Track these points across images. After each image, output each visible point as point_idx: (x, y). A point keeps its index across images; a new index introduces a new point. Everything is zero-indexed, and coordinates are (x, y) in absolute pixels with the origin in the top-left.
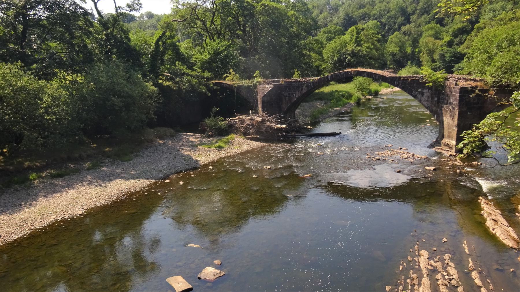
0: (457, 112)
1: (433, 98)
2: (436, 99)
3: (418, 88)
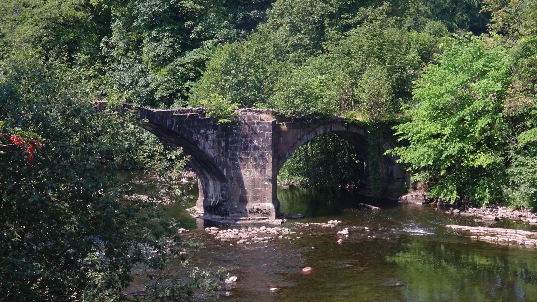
1: (219, 143)
2: (223, 144)
3: (200, 128)
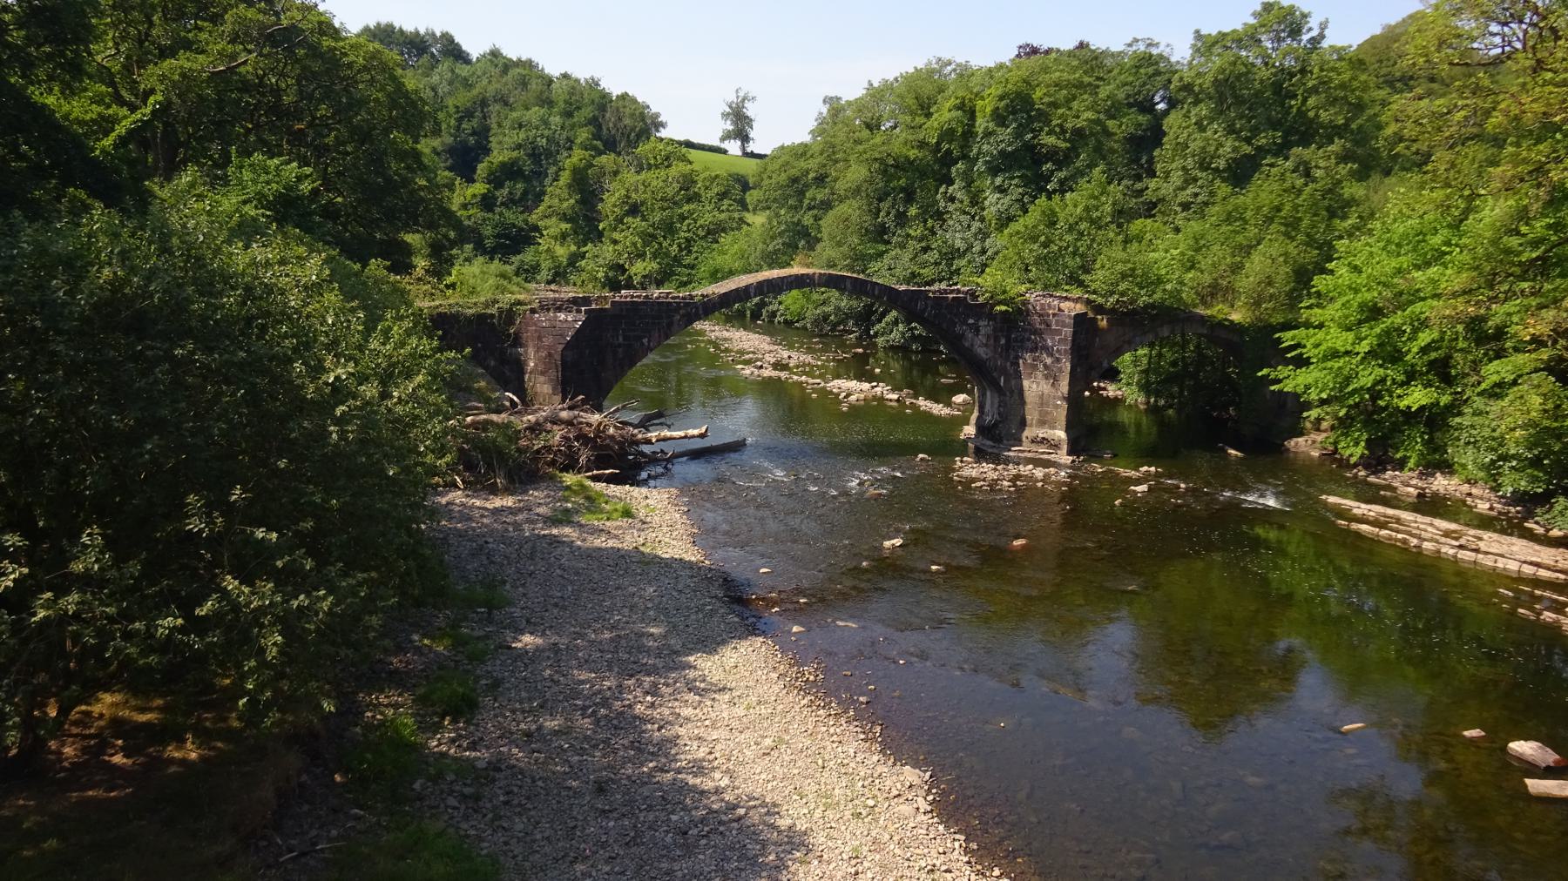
0: (1067, 366)
1: (997, 339)
3: (968, 317)
